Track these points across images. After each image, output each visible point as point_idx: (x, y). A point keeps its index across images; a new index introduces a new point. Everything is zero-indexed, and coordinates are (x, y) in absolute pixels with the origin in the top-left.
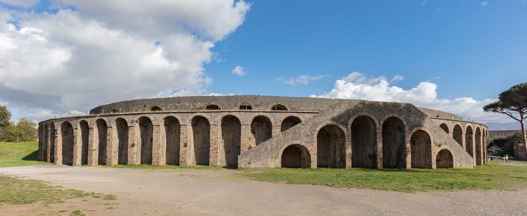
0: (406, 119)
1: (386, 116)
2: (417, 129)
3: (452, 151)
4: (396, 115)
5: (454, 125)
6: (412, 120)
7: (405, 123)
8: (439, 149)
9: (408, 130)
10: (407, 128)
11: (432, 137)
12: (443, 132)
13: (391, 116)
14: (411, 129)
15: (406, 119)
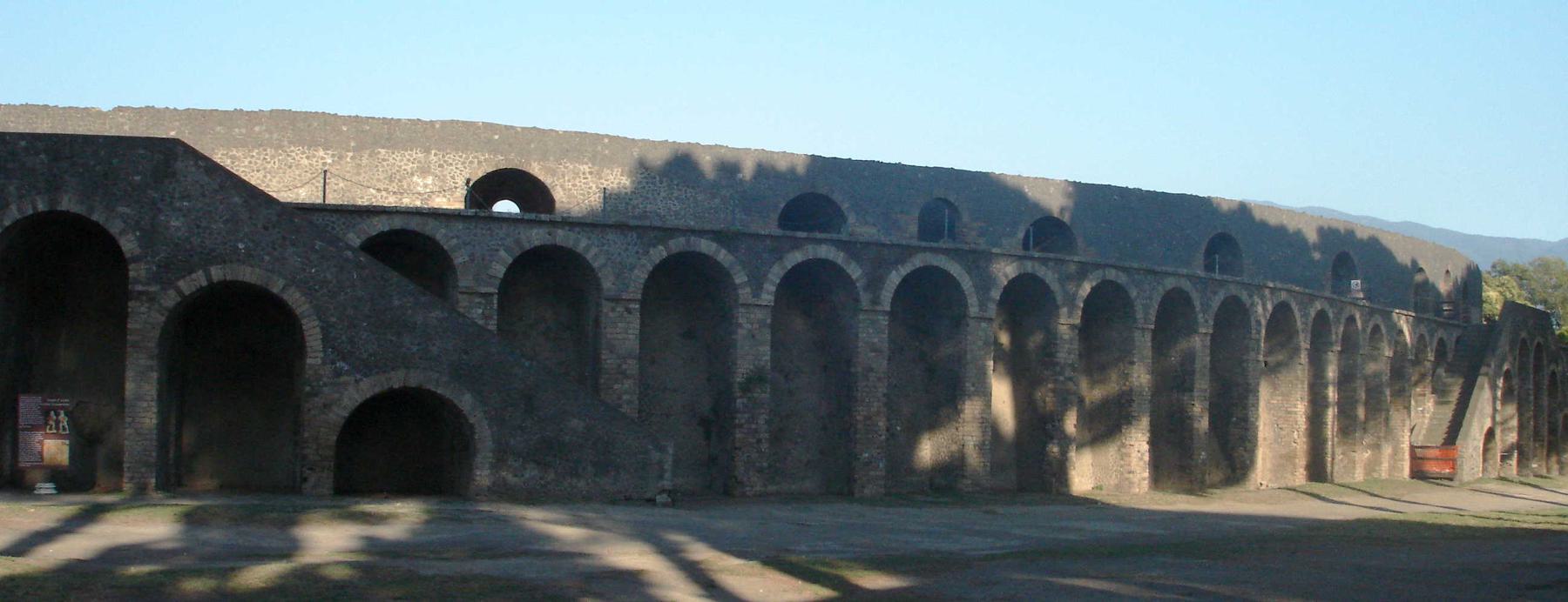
0: (137, 222)
1: (14, 207)
2: (208, 276)
3: (466, 402)
4: (68, 203)
5: (659, 253)
6: (178, 229)
7: (129, 245)
8: (357, 392)
9: (148, 284)
10: (143, 273)
11: (317, 323)
12: (401, 293)
13: (41, 207)
14: (167, 273)
15: (137, 222)
